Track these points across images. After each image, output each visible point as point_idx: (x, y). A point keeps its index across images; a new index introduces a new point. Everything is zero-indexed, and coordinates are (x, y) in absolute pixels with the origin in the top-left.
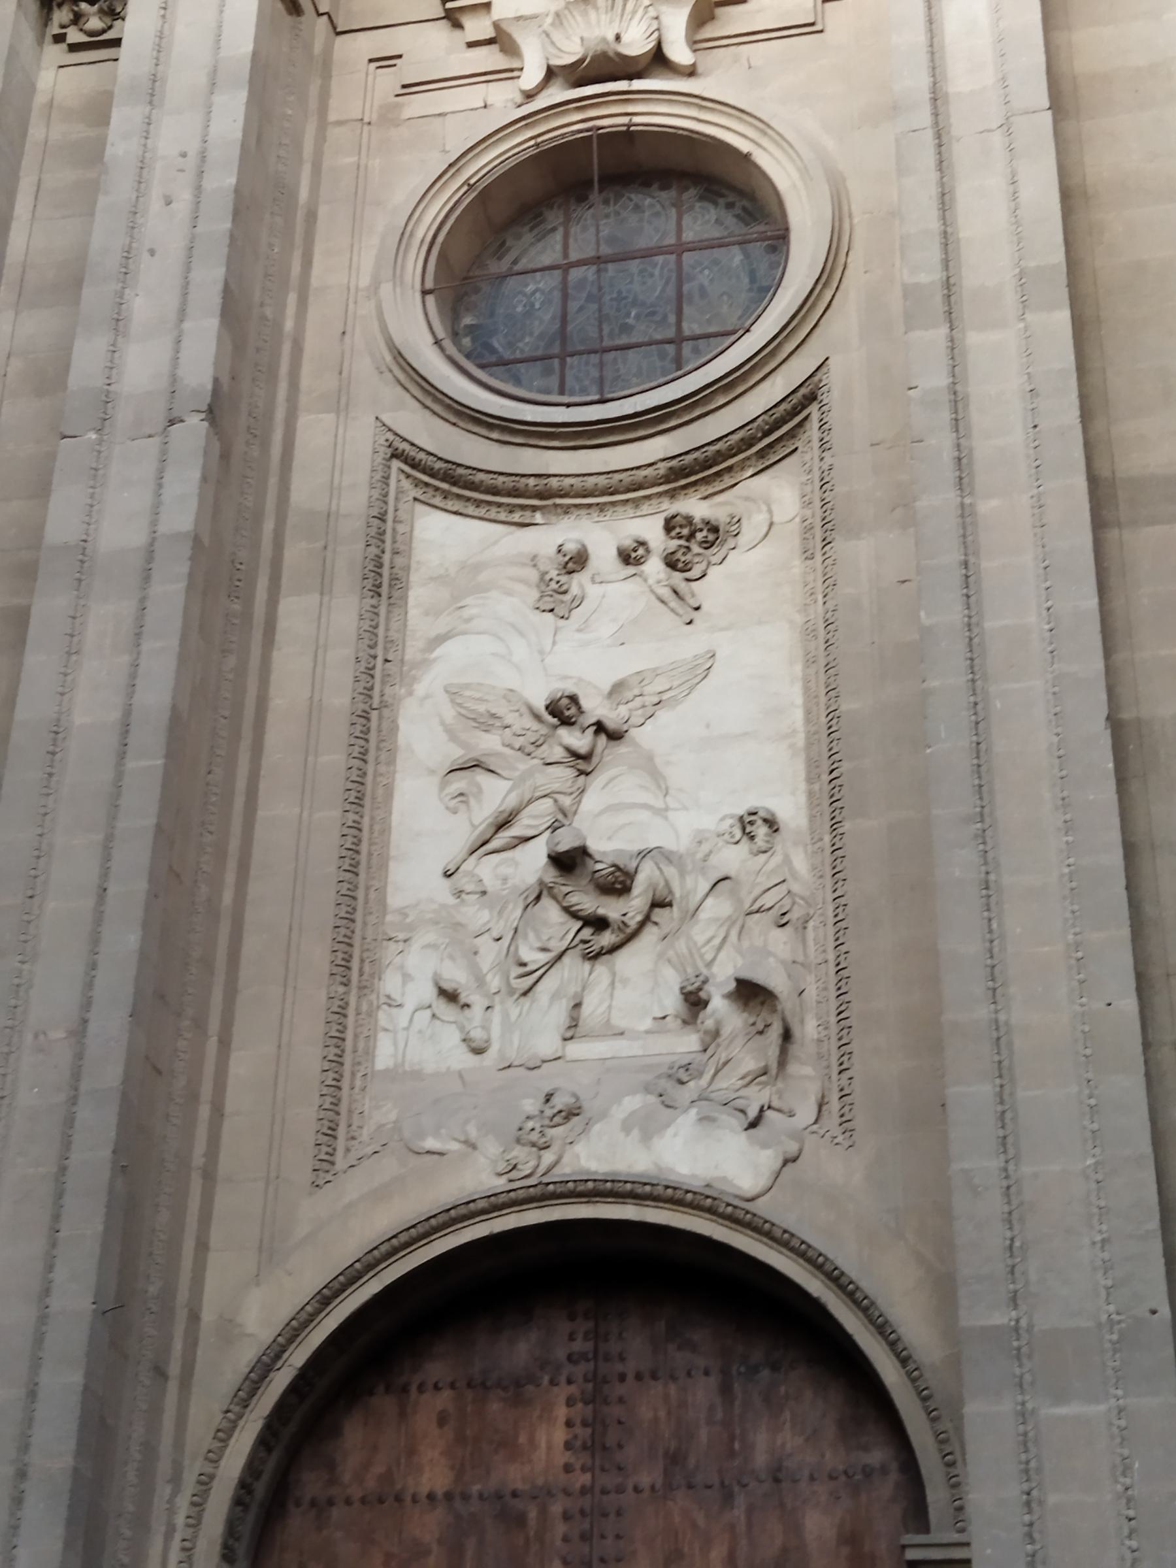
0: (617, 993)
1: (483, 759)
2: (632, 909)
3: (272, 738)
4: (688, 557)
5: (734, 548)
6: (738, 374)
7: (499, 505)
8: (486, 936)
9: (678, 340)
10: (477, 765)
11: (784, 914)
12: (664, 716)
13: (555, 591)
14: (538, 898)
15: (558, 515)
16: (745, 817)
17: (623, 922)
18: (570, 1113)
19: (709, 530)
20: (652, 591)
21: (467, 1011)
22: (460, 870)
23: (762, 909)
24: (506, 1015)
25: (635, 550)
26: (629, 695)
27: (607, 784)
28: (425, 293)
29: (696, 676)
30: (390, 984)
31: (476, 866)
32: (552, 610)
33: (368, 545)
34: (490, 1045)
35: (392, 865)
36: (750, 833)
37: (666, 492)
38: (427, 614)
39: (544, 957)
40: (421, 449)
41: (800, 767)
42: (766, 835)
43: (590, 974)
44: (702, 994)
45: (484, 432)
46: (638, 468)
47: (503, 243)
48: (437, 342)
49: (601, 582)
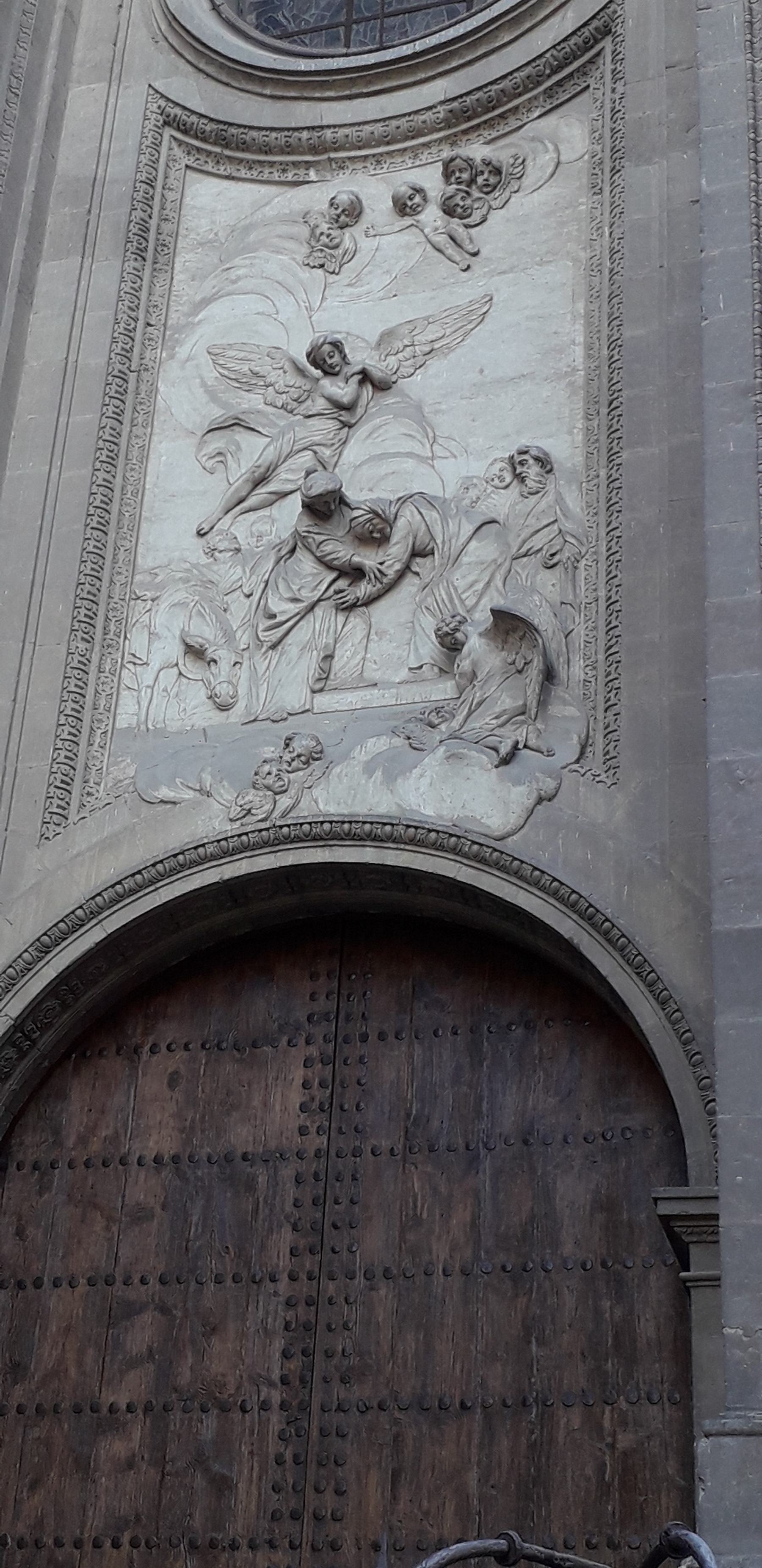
12: (435, 365)
14: (293, 551)
16: (516, 456)
25: (411, 198)
32: (322, 266)
36: (521, 473)
39: (294, 608)
41: (579, 406)
42: (538, 474)
46: (416, 112)
49: (375, 236)
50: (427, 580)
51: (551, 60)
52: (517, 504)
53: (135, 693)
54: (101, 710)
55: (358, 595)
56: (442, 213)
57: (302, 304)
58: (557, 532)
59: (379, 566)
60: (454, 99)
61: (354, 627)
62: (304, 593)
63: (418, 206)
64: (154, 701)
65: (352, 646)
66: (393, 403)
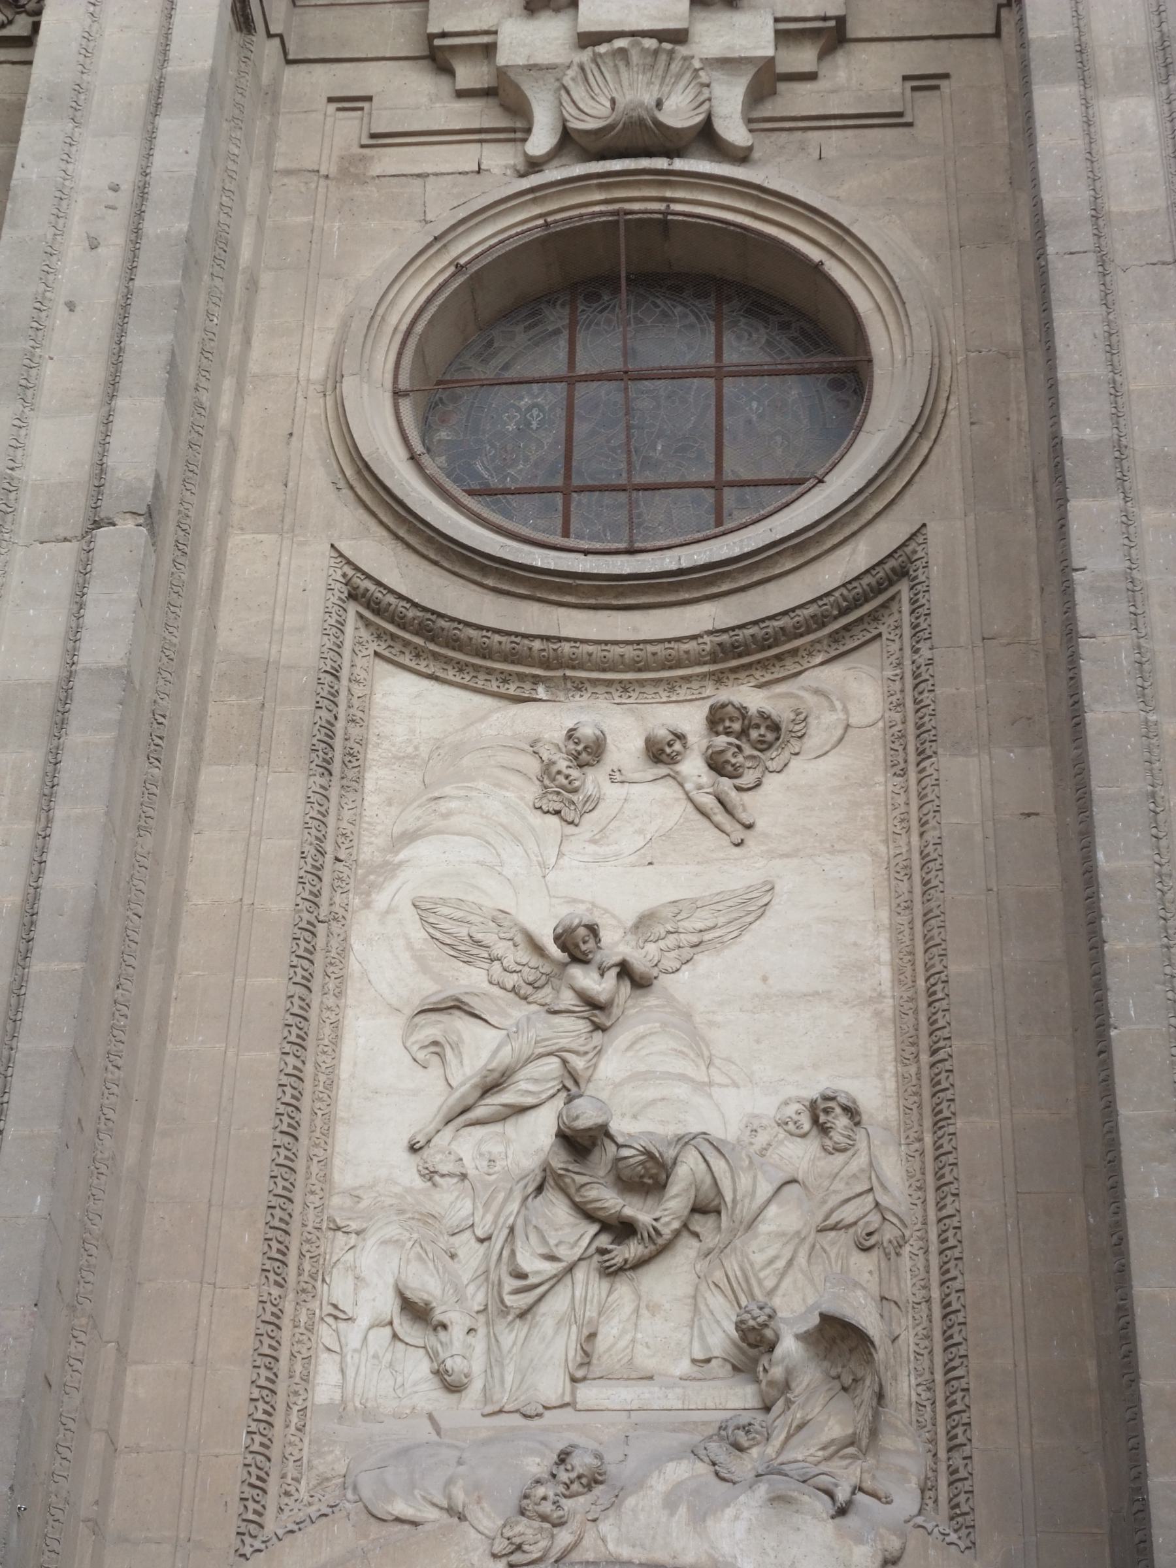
0: (645, 1322)
1: (466, 999)
3: (186, 949)
4: (740, 759)
5: (797, 754)
6: (811, 533)
7: (490, 671)
8: (467, 1235)
9: (717, 486)
10: (457, 1006)
11: (870, 1234)
12: (704, 962)
13: (563, 787)
14: (540, 1189)
16: (819, 1100)
18: (593, 1480)
19: (767, 727)
20: (690, 800)
21: (442, 1334)
22: (431, 1144)
24: (493, 1341)
26: (660, 930)
27: (634, 1043)
28: (397, 394)
29: (749, 913)
30: (339, 1289)
31: (454, 1138)
32: (557, 813)
34: (470, 1381)
35: (341, 1131)
37: (712, 674)
39: (550, 1268)
40: (391, 591)
44: (768, 1333)
45: (478, 578)
47: (490, 344)
48: (413, 458)
49: (622, 782)
50: (711, 1245)
51: (840, 600)
52: (819, 1159)
53: (337, 1358)
54: (297, 1379)
55: (627, 1256)
57: (532, 856)
58: (873, 1206)
59: (655, 1223)
62: (562, 1252)
63: (678, 754)
64: (362, 1370)
66: (657, 1006)
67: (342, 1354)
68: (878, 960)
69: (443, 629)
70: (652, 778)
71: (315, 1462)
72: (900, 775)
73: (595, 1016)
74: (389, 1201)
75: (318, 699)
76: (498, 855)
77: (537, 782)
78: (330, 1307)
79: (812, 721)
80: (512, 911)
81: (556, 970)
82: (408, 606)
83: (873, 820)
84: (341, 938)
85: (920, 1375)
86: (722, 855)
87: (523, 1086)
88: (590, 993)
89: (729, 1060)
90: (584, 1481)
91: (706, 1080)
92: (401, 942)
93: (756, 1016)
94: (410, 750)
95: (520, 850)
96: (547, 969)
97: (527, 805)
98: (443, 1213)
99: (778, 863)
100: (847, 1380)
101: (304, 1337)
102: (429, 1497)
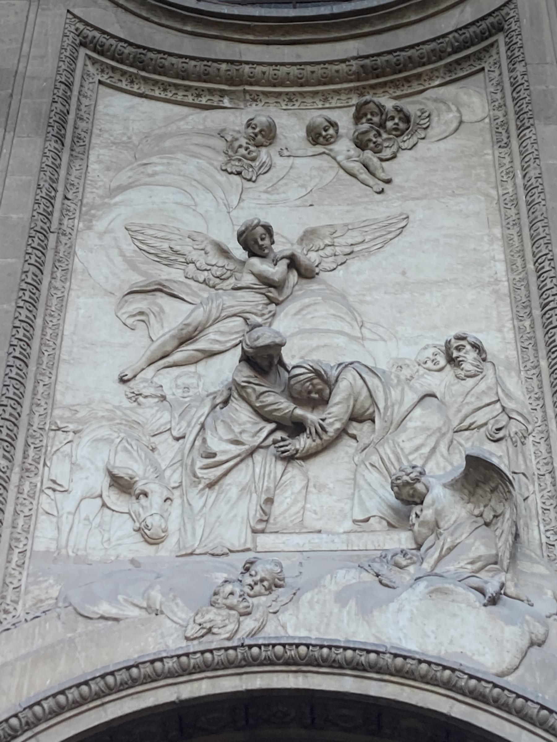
0: (311, 497)
2: (330, 416)
4: (379, 140)
5: (423, 138)
8: (167, 435)
11: (499, 430)
12: (354, 264)
14: (226, 402)
15: (245, 100)
16: (453, 340)
17: (321, 426)
19: (400, 119)
23: (473, 427)
29: (390, 232)
32: (239, 173)
33: (54, 102)
35: (63, 368)
36: (458, 357)
37: (357, 88)
38: (108, 169)
39: (235, 450)
40: (113, 36)
43: (282, 476)
45: (179, 26)
46: (331, 62)
49: (289, 156)
50: (367, 442)
52: (453, 385)
53: (55, 520)
55: (298, 447)
56: (354, 146)
57: (220, 201)
59: (321, 422)
60: (367, 57)
61: (293, 477)
62: (245, 437)
63: (332, 137)
64: (75, 529)
65: (292, 493)
66: (318, 289)
67: (59, 517)
68: (493, 258)
69: (152, 59)
70: (311, 154)
71: (31, 588)
72: (504, 147)
73: (270, 292)
74: (101, 414)
75: (55, 97)
76: (194, 199)
77: (223, 154)
78: (51, 482)
79: (435, 119)
80: (205, 232)
81: (238, 267)
82: (125, 45)
83: (484, 175)
84: (68, 246)
85: (548, 524)
86: (366, 199)
87: (212, 336)
88: (265, 274)
89: (377, 324)
90: (266, 583)
91: (360, 335)
92: (116, 251)
93: (398, 296)
94: (125, 139)
95: (210, 196)
96: (231, 267)
97: (216, 168)
98: (145, 421)
99: (411, 204)
100: (488, 515)
101: (27, 502)
102: (130, 600)
